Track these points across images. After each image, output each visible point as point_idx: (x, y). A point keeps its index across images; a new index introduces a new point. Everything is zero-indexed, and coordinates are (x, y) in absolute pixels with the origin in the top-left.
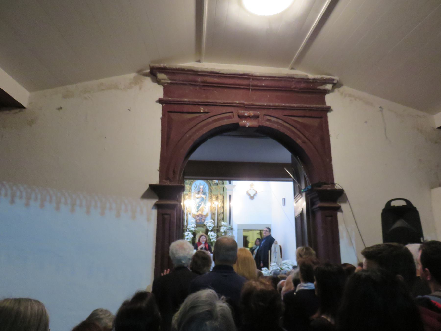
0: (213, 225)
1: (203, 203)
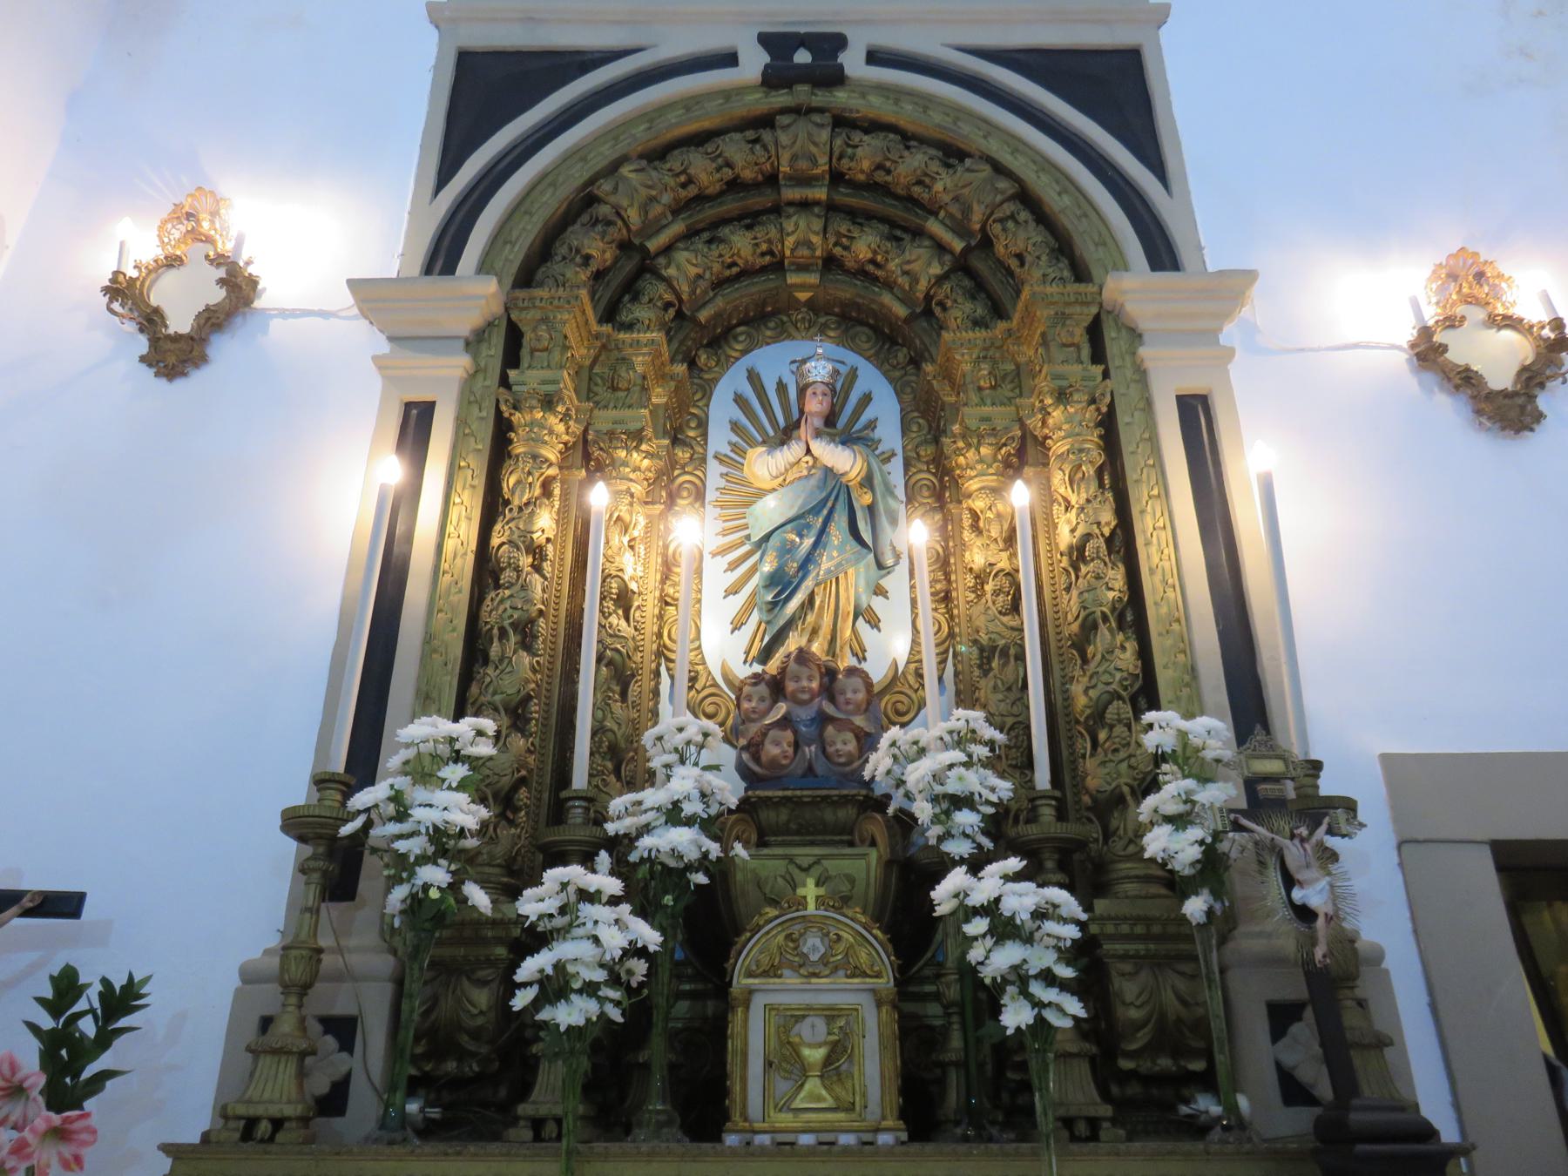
0: (1004, 788)
1: (838, 532)
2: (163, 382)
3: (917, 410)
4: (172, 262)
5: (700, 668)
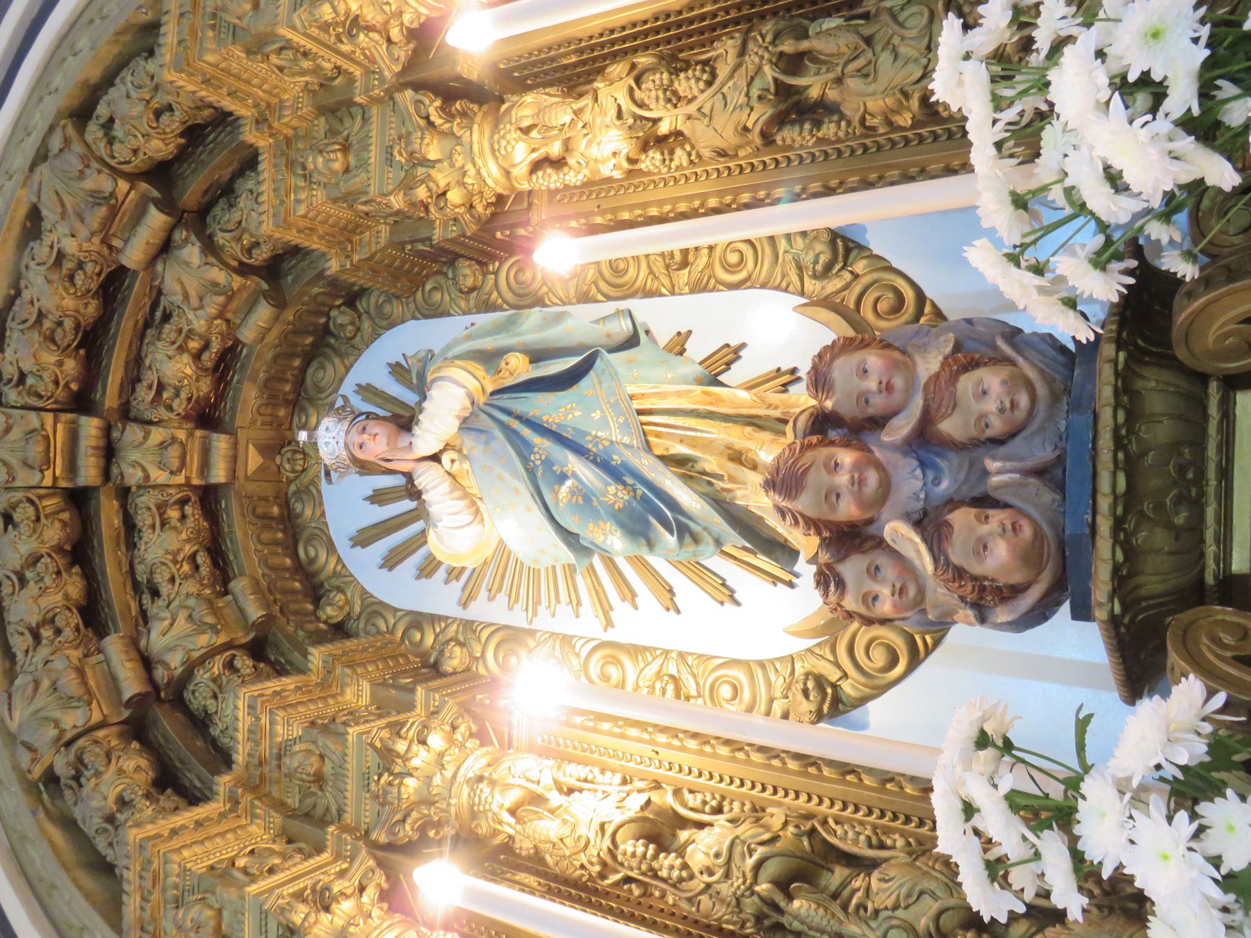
3: (414, 293)
5: (800, 670)
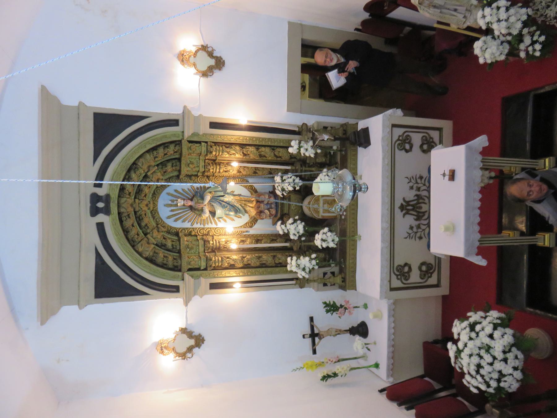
2: (205, 342)
4: (174, 349)
